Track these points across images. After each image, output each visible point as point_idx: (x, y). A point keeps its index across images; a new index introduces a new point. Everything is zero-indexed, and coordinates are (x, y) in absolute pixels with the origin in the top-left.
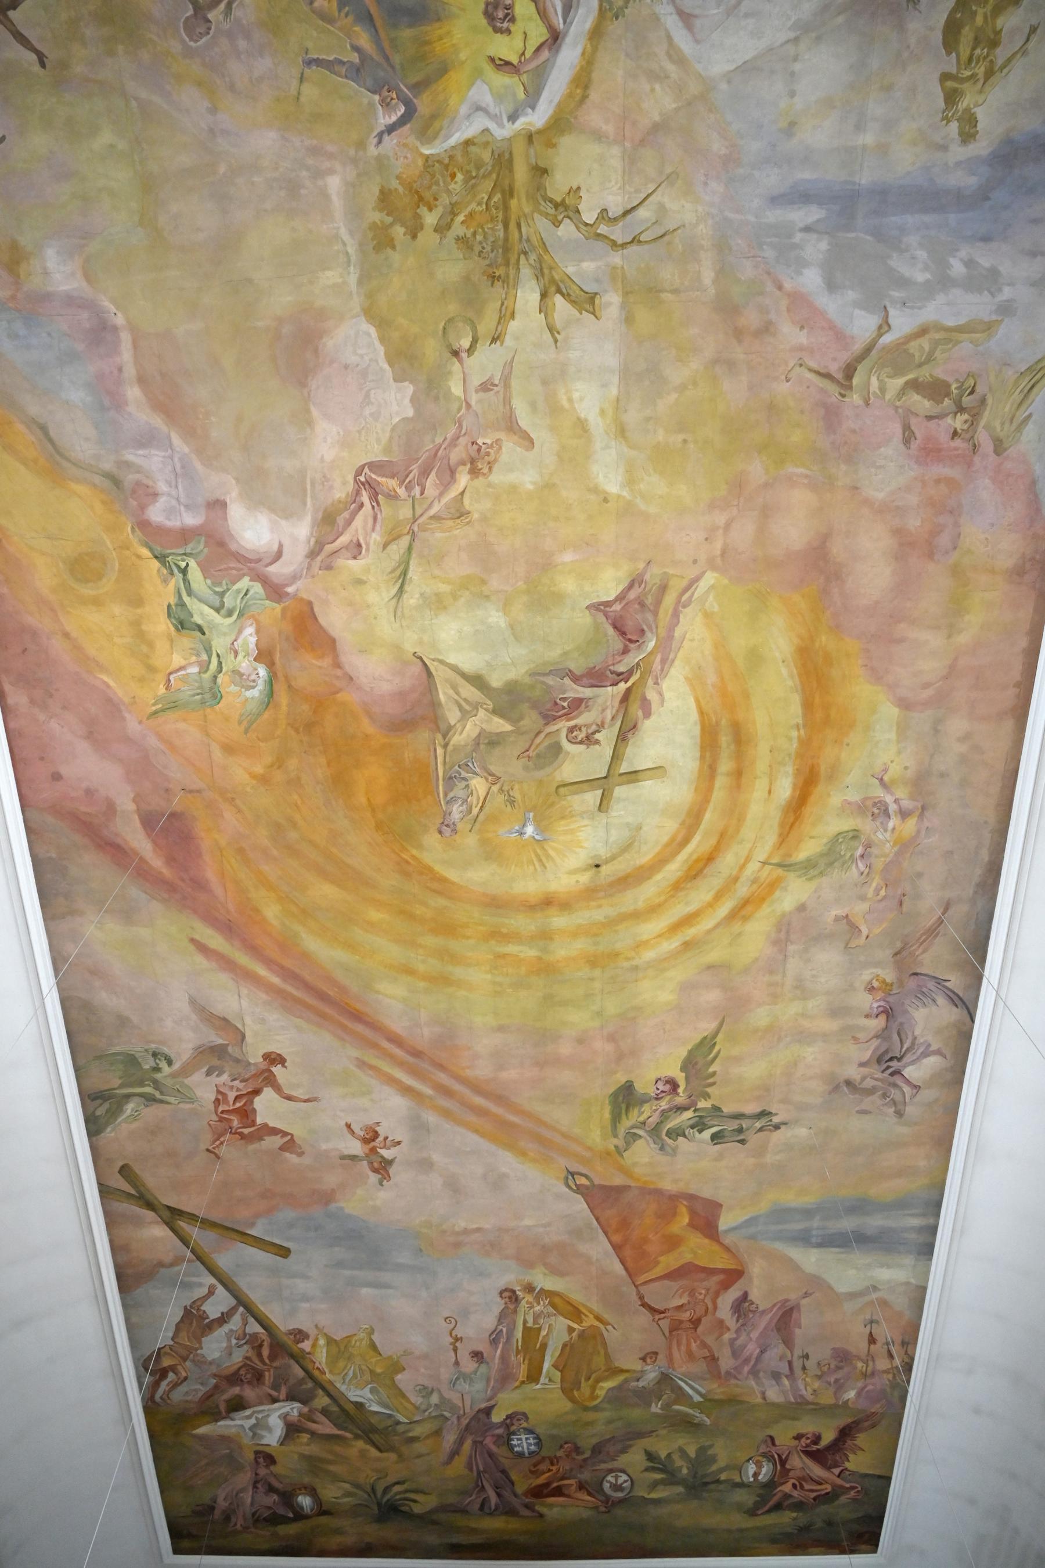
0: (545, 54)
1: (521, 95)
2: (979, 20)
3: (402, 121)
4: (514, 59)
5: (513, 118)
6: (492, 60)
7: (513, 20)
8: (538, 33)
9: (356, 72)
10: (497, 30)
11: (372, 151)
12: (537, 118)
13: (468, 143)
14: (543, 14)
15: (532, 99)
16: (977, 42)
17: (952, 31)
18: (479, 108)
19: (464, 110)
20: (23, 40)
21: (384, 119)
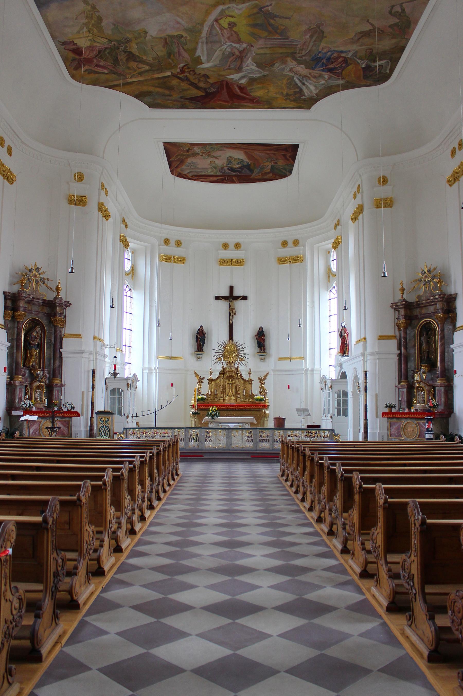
0: (219, 18)
1: (226, 12)
2: (93, 21)
3: (264, 7)
4: (228, 17)
5: (229, 8)
6: (235, 17)
7: (228, 24)
8: (222, 22)
9: (276, 16)
10: (234, 22)
11: (274, 3)
12: (220, 8)
13: (243, 3)
14: (220, 24)
15: (223, 11)
16: (92, 18)
17: (100, 19)
18: (239, 9)
19: (244, 9)
20: (371, 24)
21: (270, 8)
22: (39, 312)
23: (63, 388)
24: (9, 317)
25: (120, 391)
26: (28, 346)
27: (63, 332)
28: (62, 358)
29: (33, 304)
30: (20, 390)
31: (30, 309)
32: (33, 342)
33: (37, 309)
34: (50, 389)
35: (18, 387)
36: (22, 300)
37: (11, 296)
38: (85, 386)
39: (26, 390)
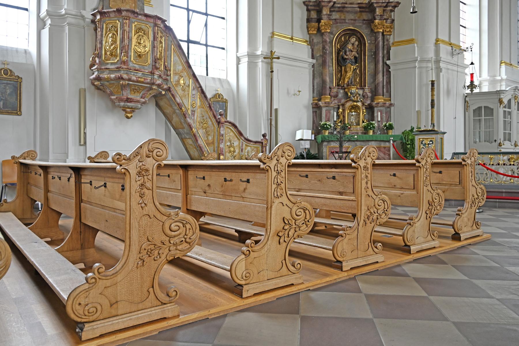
22: (355, 20)
23: (392, 108)
24: (314, 30)
25: (489, 111)
26: (341, 62)
27: (391, 41)
28: (390, 72)
29: (348, 12)
30: (328, 112)
31: (343, 17)
32: (347, 55)
33: (352, 17)
34: (370, 109)
35: (324, 110)
36: (325, 6)
37: (314, 6)
38: (420, 102)
39: (338, 113)
